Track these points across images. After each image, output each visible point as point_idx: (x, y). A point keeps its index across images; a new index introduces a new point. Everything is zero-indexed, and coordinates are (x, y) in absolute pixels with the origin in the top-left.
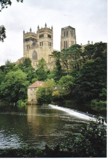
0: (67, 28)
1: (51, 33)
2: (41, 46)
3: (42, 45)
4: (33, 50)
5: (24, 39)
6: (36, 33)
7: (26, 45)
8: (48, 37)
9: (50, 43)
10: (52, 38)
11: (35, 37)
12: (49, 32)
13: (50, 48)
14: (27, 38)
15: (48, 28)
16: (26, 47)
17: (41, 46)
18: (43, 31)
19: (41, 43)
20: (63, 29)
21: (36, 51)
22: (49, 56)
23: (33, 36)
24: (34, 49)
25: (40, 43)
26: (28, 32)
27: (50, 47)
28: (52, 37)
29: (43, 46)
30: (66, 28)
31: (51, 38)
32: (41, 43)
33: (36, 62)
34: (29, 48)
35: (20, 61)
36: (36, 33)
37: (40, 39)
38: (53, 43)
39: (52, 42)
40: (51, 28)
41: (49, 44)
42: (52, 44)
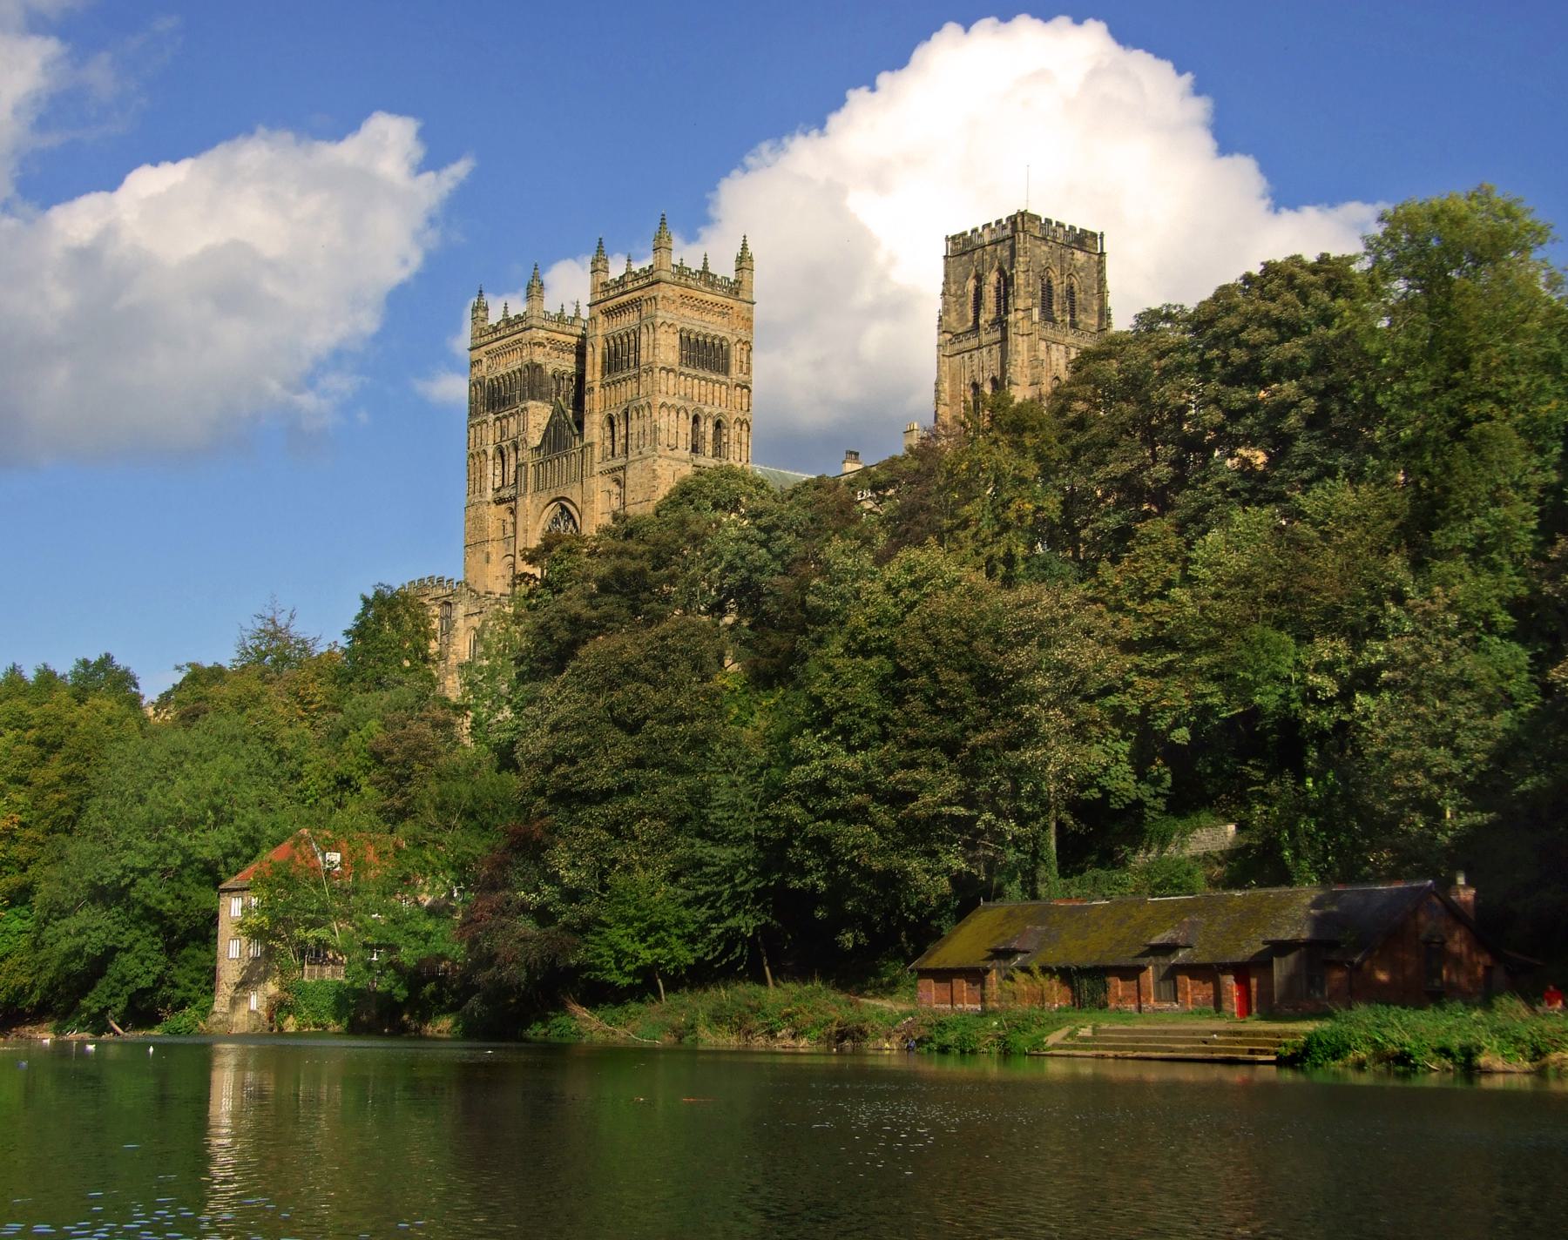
7: (490, 452)
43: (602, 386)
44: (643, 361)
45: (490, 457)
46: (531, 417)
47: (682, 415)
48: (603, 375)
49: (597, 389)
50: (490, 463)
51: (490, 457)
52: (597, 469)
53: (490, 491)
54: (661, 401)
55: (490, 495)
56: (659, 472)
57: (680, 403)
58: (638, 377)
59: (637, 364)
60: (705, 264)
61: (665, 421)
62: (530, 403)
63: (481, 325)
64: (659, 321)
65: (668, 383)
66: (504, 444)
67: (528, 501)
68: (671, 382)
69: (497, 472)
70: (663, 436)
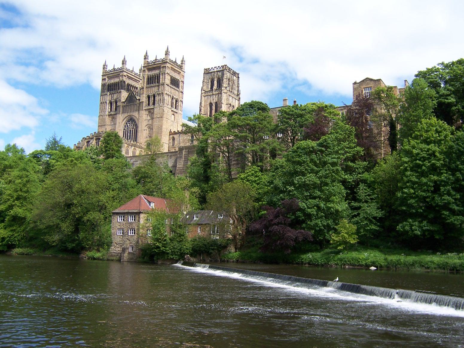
0: (219, 69)
1: (179, 73)
2: (149, 105)
3: (154, 104)
4: (126, 115)
5: (103, 85)
6: (137, 71)
7: (108, 102)
8: (171, 83)
9: (176, 101)
10: (180, 88)
11: (136, 81)
12: (175, 71)
13: (175, 114)
14: (112, 81)
15: (172, 61)
16: (108, 107)
17: (149, 105)
18: (159, 68)
19: (152, 99)
20: (207, 72)
21: (135, 118)
22: (171, 136)
23: (129, 78)
24: (129, 114)
25: (149, 97)
26: (116, 67)
27: (174, 109)
28: (181, 84)
29: (156, 105)
30: (216, 70)
31: (178, 86)
32: (152, 99)
33: (133, 148)
34: (116, 109)
35: (89, 141)
36: (137, 71)
37: (149, 86)
38: (182, 101)
39: (180, 99)
40: (179, 62)
41: (172, 103)
42: (180, 103)
43: (146, 87)
44: (161, 82)
45: (108, 103)
46: (122, 94)
47: (170, 97)
48: (147, 85)
49: (145, 88)
50: (108, 105)
51: (108, 103)
52: (144, 108)
53: (107, 112)
54: (166, 92)
55: (107, 113)
56: (165, 110)
57: (170, 94)
58: (158, 86)
59: (158, 82)
60: (176, 60)
61: (166, 97)
62: (122, 91)
63: (106, 70)
64: (166, 72)
65: (167, 88)
66: (112, 101)
67: (120, 115)
68: (168, 88)
69: (109, 108)
70: (166, 101)
